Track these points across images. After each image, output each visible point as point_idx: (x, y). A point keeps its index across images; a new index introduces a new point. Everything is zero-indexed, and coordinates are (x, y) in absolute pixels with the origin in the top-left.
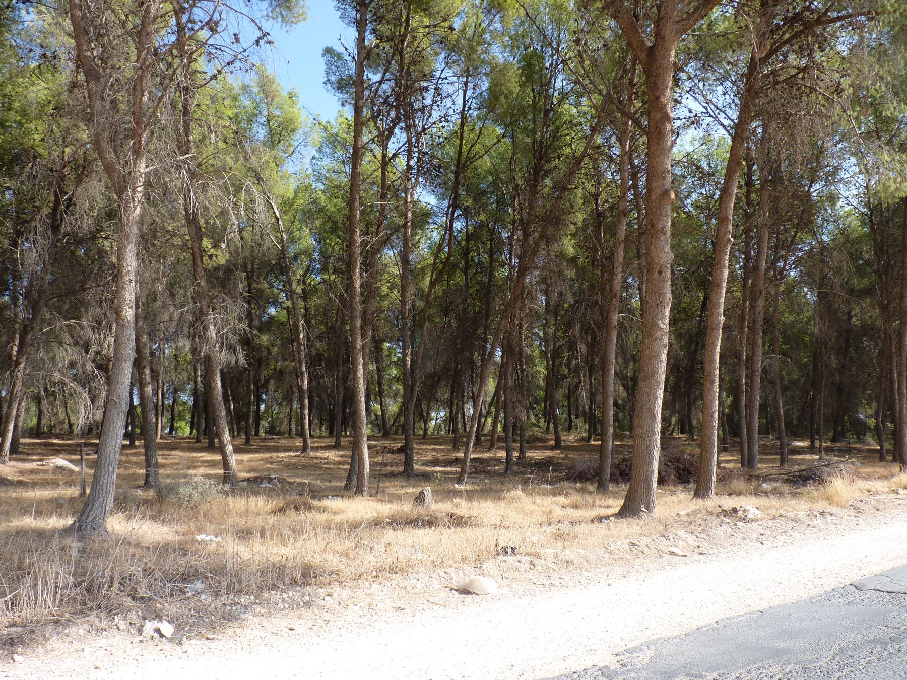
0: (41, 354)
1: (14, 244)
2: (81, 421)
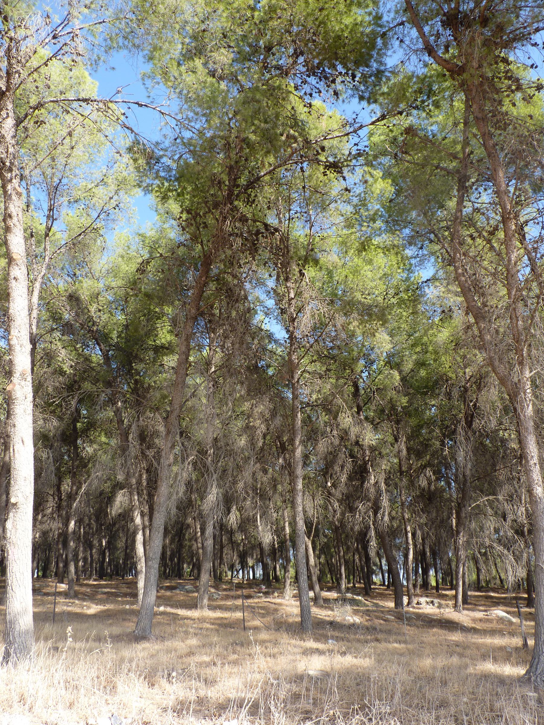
0: (473, 525)
1: (443, 444)
2: (511, 579)
